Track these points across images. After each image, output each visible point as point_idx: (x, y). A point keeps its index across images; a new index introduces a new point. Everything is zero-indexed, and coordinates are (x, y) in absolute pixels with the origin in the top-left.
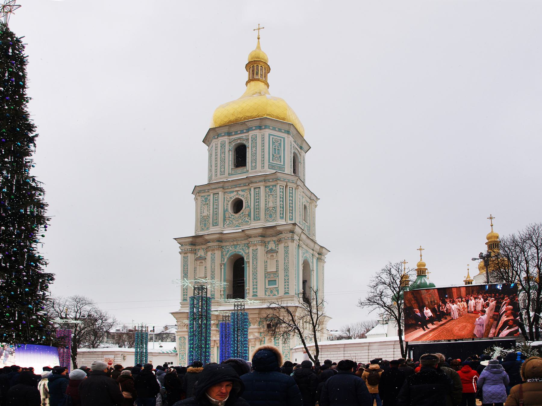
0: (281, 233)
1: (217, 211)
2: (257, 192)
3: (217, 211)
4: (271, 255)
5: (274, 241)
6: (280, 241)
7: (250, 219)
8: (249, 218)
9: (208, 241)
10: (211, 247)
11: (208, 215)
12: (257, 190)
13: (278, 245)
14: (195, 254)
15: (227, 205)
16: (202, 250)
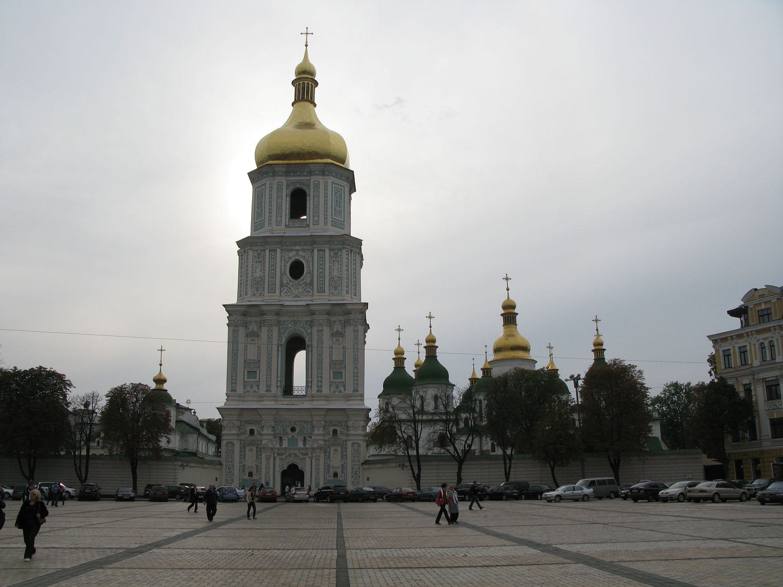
0: (350, 313)
1: (273, 273)
2: (321, 256)
3: (273, 273)
4: (336, 339)
5: (340, 321)
6: (346, 323)
7: (311, 289)
8: (311, 288)
9: (263, 314)
10: (267, 321)
11: (261, 276)
12: (322, 253)
13: (345, 326)
14: (246, 327)
15: (285, 266)
16: (255, 324)
